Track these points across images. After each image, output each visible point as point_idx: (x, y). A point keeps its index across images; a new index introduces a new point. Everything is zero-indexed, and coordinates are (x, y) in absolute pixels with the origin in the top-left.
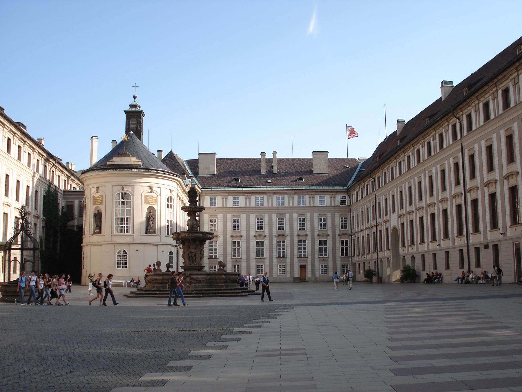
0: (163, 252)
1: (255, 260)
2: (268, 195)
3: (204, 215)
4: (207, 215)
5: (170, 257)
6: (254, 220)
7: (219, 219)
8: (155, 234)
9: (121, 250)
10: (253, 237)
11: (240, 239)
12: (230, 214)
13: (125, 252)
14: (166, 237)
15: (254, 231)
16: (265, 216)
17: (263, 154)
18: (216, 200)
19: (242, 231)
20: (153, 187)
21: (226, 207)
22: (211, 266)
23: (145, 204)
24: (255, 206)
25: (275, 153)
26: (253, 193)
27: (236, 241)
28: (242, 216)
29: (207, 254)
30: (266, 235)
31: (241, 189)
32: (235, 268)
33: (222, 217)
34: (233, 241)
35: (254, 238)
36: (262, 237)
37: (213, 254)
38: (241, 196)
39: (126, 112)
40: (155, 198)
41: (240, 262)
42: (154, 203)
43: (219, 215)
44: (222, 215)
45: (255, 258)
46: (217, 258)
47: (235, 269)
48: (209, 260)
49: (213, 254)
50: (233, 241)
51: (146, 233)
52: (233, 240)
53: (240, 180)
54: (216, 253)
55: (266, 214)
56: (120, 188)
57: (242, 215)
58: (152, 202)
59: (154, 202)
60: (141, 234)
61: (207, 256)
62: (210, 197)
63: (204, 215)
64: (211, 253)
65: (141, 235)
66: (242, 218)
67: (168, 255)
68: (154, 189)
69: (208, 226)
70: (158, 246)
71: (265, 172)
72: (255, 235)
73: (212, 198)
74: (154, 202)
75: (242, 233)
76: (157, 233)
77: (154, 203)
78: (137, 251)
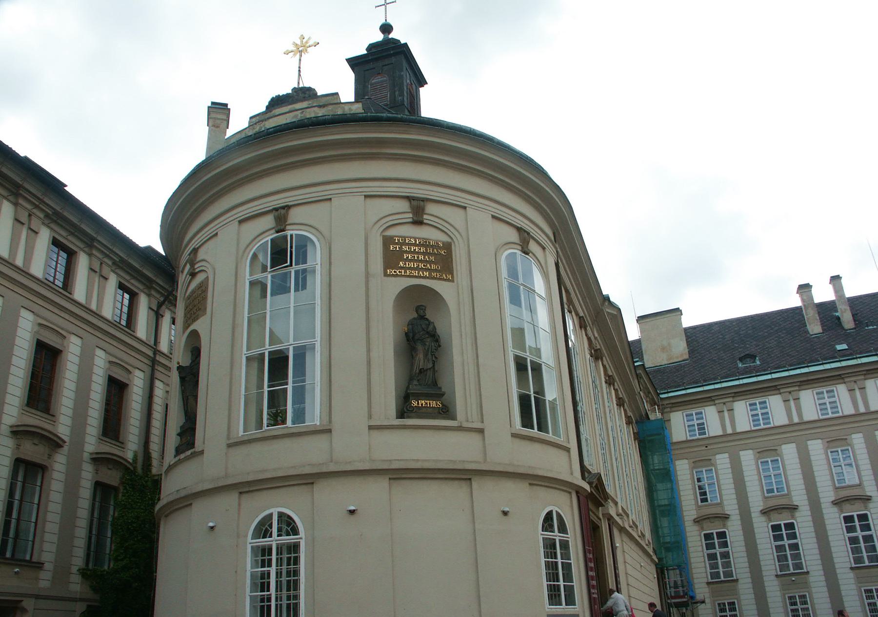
0: (505, 513)
1: (851, 575)
2: (850, 382)
3: (677, 463)
4: (686, 461)
5: (550, 545)
6: (823, 456)
7: (719, 467)
8: (453, 418)
9: (271, 515)
10: (830, 505)
11: (793, 517)
12: (751, 452)
13: (288, 525)
14: (514, 435)
15: (831, 488)
16: (855, 441)
17: (804, 289)
18: (702, 418)
19: (793, 493)
20: (424, 200)
21: (735, 434)
22: (719, 604)
23: (386, 275)
24: (815, 418)
25: (835, 280)
26: (806, 382)
27: (780, 524)
28: (784, 452)
29: (703, 570)
30: (869, 494)
31: (769, 377)
32: (795, 604)
33: (728, 461)
34: (772, 526)
35: (835, 509)
36: (858, 505)
37: (721, 570)
38: (769, 397)
39: (355, 63)
40: (440, 248)
41: (806, 585)
42: (436, 270)
43: (718, 456)
44: (726, 455)
45: (852, 568)
46: (735, 578)
47: (793, 607)
48: (712, 586)
49: (721, 570)
50: (772, 526)
51: (401, 415)
52: (770, 521)
53: (760, 360)
54: (727, 565)
55: (854, 436)
56: (269, 221)
57: (784, 447)
58: (421, 265)
59: (433, 267)
60: (373, 423)
61: (704, 575)
62: (684, 414)
63: (677, 463)
64: (714, 566)
65: (371, 428)
66: (785, 457)
67: (540, 535)
68: (431, 208)
69: (691, 492)
70: (475, 484)
71: (822, 332)
72: (833, 499)
73: (692, 415)
74: (433, 267)
75: (794, 499)
76: (459, 417)
77: (436, 270)
78: (352, 518)
